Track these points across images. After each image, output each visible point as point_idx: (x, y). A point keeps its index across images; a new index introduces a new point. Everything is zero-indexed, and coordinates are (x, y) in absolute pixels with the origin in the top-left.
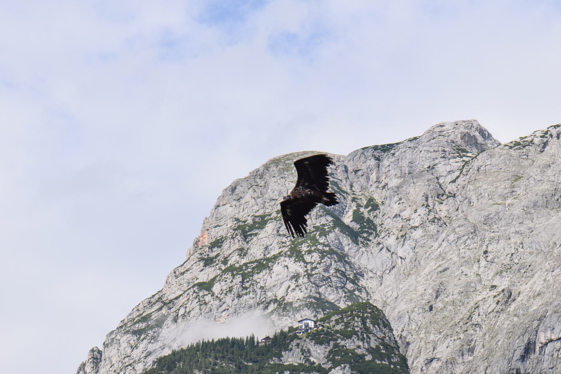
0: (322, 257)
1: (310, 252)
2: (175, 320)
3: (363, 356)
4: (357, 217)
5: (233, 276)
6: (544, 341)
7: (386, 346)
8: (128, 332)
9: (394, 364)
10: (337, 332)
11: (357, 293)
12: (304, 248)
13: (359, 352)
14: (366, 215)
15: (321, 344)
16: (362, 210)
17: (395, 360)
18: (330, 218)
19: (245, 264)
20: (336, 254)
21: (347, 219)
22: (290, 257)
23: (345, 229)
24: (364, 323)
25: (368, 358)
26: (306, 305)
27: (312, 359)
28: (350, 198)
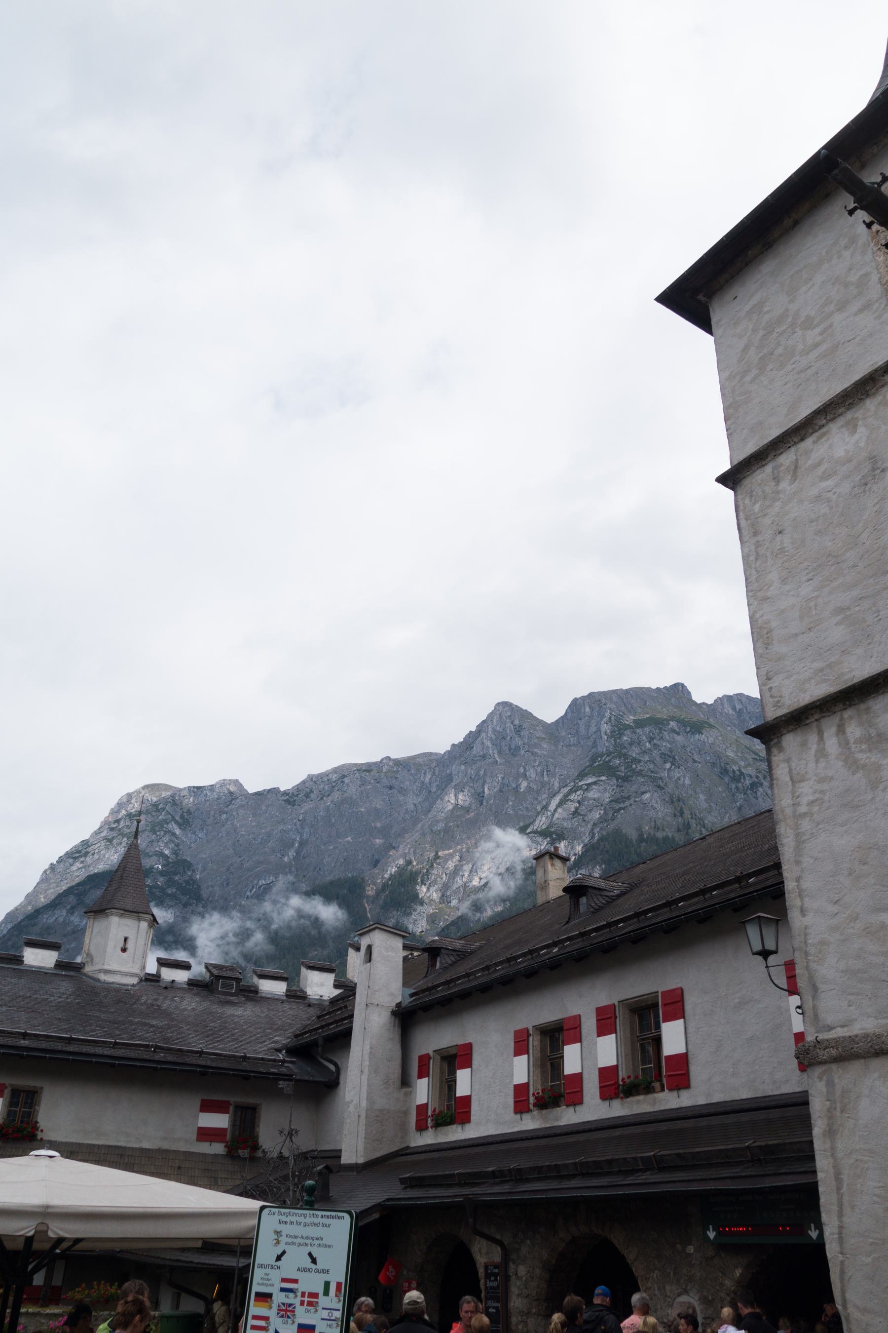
0: (165, 834)
1: (159, 831)
2: (93, 854)
3: (181, 884)
4: (182, 817)
5: (123, 838)
6: (260, 883)
7: (192, 880)
8: (69, 857)
9: (195, 889)
10: (171, 872)
11: (178, 851)
12: (157, 828)
13: (180, 881)
14: (186, 817)
15: (164, 876)
16: (184, 814)
17: (195, 887)
18: (170, 816)
19: (129, 833)
20: (171, 832)
21: (177, 818)
22: (150, 832)
23: (177, 822)
24: (184, 869)
25: (184, 885)
26: (155, 855)
27: (159, 883)
28: (180, 807)
